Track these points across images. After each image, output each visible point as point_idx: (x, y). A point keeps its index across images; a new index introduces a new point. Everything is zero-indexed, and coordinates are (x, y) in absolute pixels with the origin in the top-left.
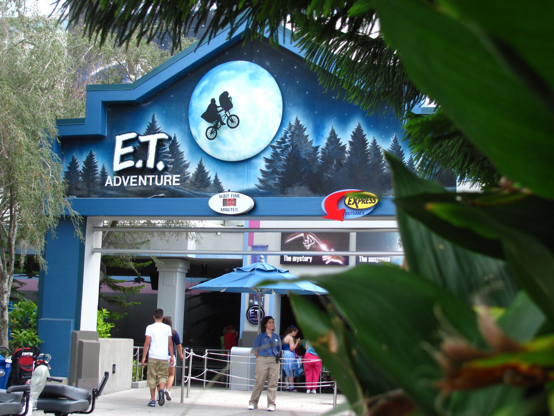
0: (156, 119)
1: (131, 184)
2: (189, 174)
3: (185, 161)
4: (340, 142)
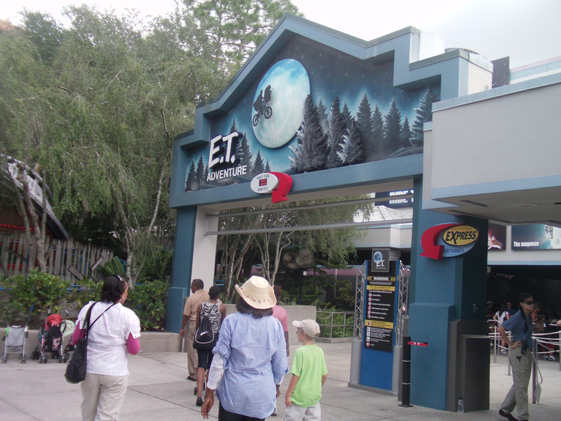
0: (235, 123)
1: (221, 178)
2: (251, 163)
3: (250, 153)
4: (350, 115)
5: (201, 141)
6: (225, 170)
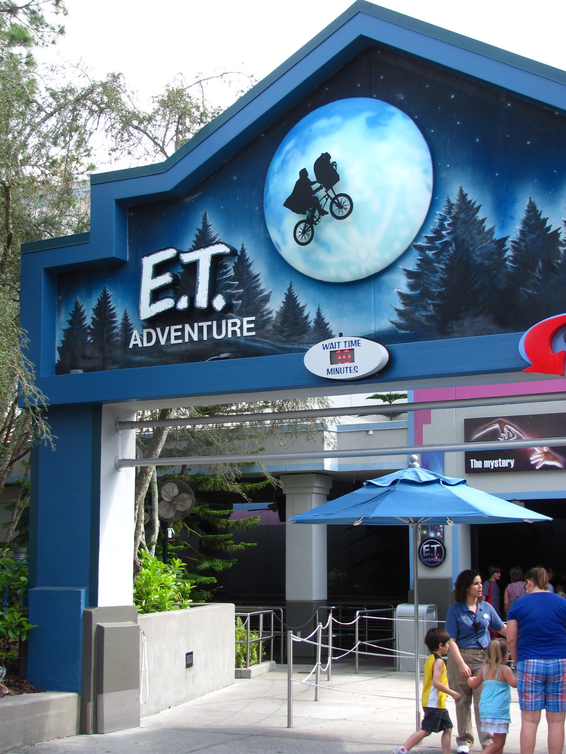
0: (209, 223)
1: (173, 341)
2: (270, 312)
3: (262, 291)
4: (547, 225)
5: (113, 259)
6: (187, 327)
